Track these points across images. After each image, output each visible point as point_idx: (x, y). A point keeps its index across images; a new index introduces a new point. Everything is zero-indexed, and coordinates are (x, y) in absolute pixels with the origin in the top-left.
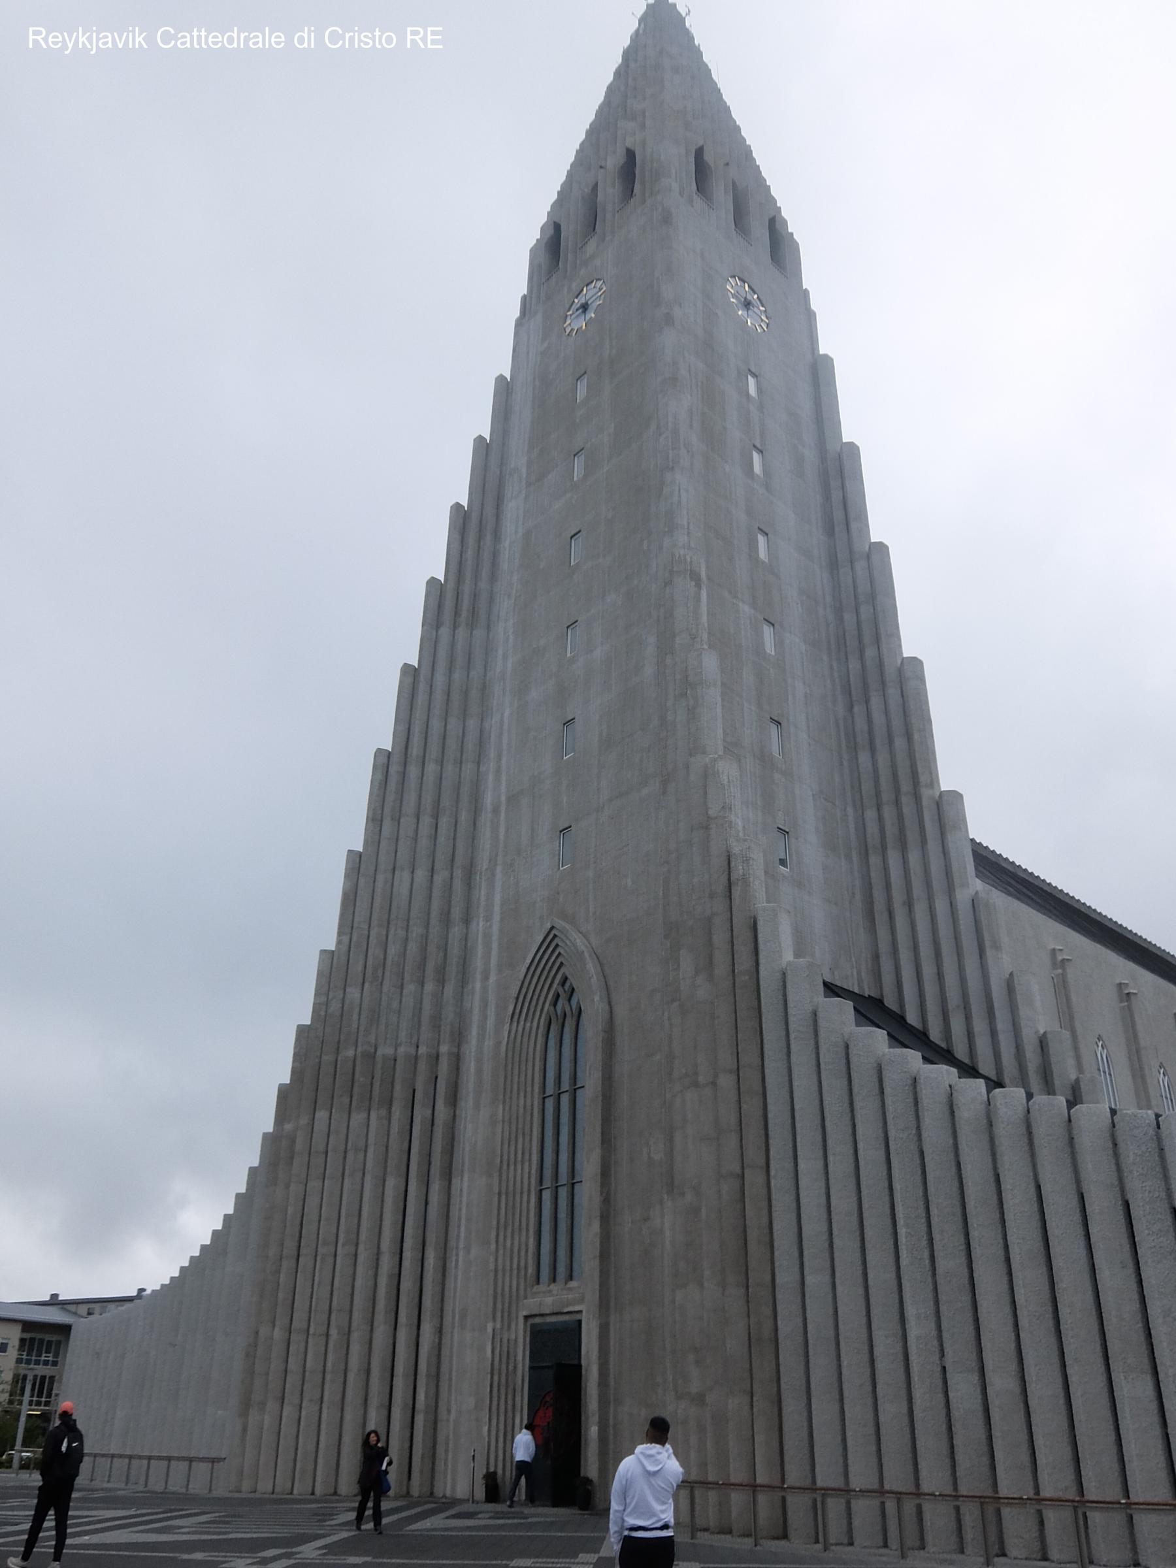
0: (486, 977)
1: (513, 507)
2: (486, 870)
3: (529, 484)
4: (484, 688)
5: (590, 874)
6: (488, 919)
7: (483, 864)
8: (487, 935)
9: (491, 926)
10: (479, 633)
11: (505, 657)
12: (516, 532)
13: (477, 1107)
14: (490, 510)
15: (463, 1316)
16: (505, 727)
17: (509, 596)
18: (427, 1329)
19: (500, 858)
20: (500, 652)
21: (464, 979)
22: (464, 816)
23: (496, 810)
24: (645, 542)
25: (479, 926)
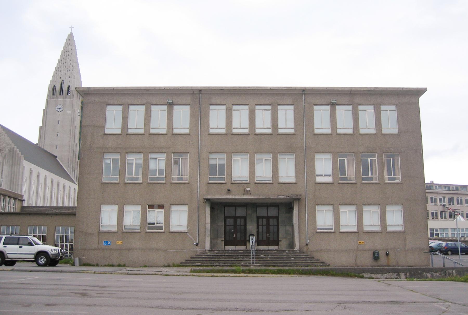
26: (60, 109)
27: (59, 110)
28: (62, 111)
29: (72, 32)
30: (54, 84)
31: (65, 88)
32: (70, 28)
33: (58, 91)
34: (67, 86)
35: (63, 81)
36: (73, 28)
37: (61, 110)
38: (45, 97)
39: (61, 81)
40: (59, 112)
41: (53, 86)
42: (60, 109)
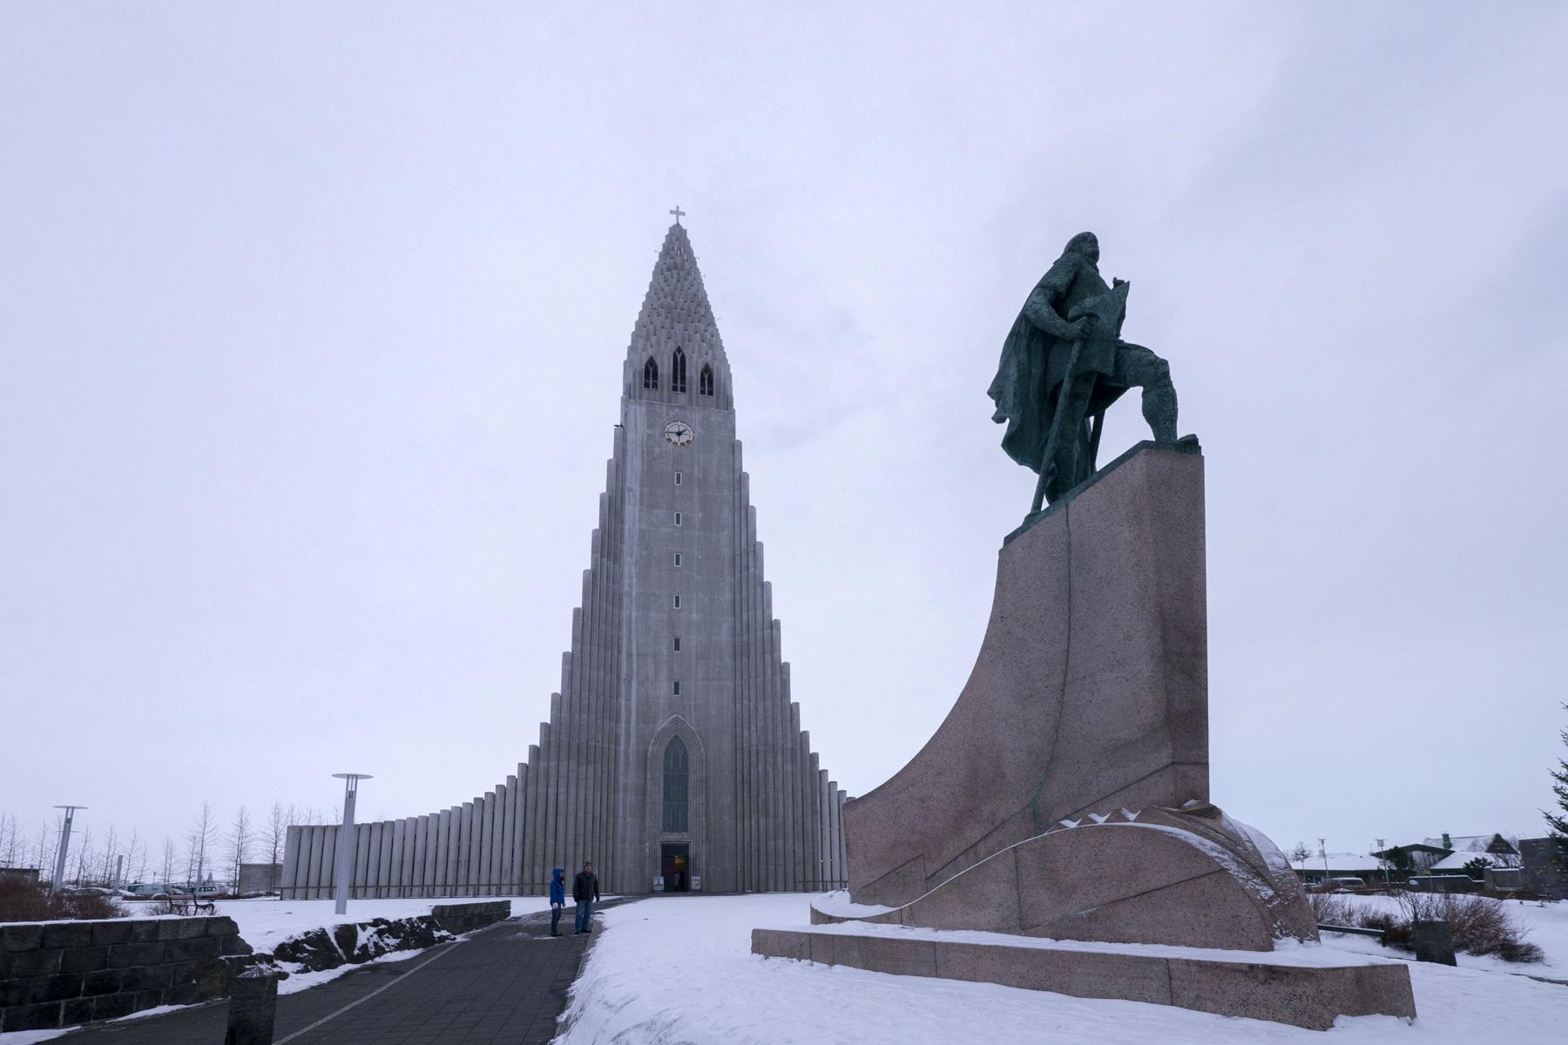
0: (628, 722)
1: (631, 511)
2: (625, 680)
3: (641, 504)
4: (621, 596)
5: (693, 703)
6: (628, 699)
7: (623, 676)
8: (628, 708)
9: (630, 704)
10: (617, 567)
11: (630, 585)
12: (634, 525)
13: (627, 770)
14: (619, 503)
15: (624, 840)
16: (634, 620)
17: (631, 556)
18: (610, 842)
19: (634, 678)
20: (626, 581)
21: (617, 722)
22: (616, 653)
23: (630, 655)
24: (721, 583)
25: (623, 701)
26: (681, 436)
27: (675, 438)
28: (688, 442)
29: (681, 223)
30: (651, 352)
31: (693, 373)
32: (672, 212)
33: (669, 376)
34: (700, 367)
35: (679, 350)
36: (683, 214)
37: (684, 439)
38: (619, 391)
39: (672, 347)
40: (675, 443)
41: (645, 359)
42: (679, 434)
